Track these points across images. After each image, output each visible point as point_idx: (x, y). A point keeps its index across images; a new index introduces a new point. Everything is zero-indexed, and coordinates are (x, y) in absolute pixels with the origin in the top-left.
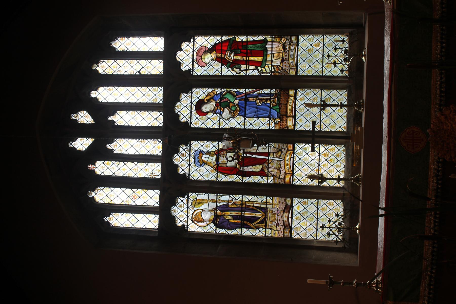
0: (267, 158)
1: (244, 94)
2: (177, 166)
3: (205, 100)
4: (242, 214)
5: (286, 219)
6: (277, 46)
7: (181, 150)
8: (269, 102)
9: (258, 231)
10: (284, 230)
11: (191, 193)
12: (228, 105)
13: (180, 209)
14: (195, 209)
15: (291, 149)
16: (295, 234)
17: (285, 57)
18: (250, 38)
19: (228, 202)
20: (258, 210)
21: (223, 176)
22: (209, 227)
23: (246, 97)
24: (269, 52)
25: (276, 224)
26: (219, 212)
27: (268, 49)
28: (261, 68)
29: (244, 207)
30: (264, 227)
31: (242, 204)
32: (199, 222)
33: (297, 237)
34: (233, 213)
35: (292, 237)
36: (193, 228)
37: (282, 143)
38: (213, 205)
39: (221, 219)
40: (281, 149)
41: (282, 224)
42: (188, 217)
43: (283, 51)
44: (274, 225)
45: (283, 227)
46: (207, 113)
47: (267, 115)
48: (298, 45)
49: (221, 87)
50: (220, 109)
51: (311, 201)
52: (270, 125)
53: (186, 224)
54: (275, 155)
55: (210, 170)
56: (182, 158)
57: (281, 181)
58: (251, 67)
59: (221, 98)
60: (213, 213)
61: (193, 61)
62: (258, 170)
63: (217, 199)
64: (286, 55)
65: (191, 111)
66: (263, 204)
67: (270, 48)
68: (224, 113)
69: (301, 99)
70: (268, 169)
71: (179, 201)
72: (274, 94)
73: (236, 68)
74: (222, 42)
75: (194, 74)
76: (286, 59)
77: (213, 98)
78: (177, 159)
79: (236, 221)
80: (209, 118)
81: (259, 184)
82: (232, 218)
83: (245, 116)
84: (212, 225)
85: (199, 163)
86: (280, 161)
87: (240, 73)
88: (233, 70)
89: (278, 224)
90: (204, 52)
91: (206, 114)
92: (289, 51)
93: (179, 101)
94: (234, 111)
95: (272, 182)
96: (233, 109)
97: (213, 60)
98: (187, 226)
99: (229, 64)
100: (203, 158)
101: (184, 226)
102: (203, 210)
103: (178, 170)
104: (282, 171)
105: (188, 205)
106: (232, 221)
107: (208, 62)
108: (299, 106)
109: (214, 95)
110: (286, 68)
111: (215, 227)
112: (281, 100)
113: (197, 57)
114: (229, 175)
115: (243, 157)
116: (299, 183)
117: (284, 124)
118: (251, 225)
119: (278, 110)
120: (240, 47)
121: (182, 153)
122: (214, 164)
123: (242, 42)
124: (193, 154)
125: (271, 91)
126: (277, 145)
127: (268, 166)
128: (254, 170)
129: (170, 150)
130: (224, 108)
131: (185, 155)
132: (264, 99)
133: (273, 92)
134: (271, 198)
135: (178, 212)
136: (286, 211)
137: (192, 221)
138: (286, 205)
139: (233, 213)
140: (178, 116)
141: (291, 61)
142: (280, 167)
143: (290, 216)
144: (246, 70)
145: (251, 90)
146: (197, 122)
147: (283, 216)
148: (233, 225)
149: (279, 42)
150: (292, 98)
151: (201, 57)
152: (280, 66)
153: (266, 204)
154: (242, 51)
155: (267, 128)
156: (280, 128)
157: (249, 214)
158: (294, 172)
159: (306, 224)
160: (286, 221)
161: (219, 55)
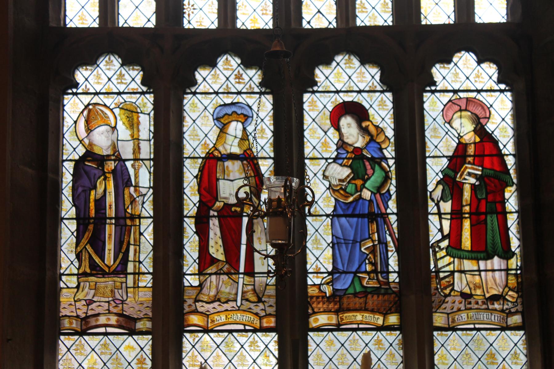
0: (242, 270)
1: (384, 211)
2: (213, 65)
3: (367, 123)
4: (111, 218)
5: (102, 320)
6: (498, 281)
7: (251, 72)
8: (369, 268)
9: (73, 256)
10: (78, 316)
11: (152, 100)
12: (359, 174)
13: (115, 77)
14: (117, 111)
15: (265, 325)
16: (68, 343)
17: (473, 301)
18: (512, 220)
19: (136, 186)
20: (121, 256)
21: (196, 172)
22: (75, 143)
23: (377, 217)
24: (482, 265)
25: (90, 297)
26: (111, 165)
27: (489, 262)
28: (447, 248)
29: (126, 222)
30: (81, 271)
31: (133, 217)
32: (87, 121)
33: (62, 349)
34: (111, 199)
35: (62, 337)
36: (73, 107)
37: (277, 303)
38: (127, 152)
39: (96, 172)
40: (263, 302)
41: (90, 313)
42: (96, 94)
43: (487, 295)
44: (87, 293)
45: (83, 316)
46: (338, 128)
47: (340, 267)
48: (503, 329)
49: (398, 159)
50: (349, 159)
52: (317, 273)
53: (80, 91)
54: (250, 288)
55: (208, 142)
56: (233, 76)
57: (190, 305)
58: (446, 225)
59: (373, 160)
60: (110, 152)
61: (455, 92)
62: (212, 251)
63: (142, 160)
64: (477, 303)
65: (341, 91)
66: (135, 266)
67: (492, 264)
68: (339, 168)
69: (379, 342)
70: (215, 274)
71: (134, 73)
72: (388, 279)
73: (443, 191)
74: (501, 156)
75: (426, 95)
76: (470, 303)
77: (372, 140)
78: (228, 64)
79: (92, 205)
80: (326, 133)
81: (179, 255)
82: (98, 197)
83: (335, 215)
84: (81, 151)
85: (221, 114)
86: (236, 301)
87: (433, 200)
88: (438, 183)
89: (89, 302)
90: (476, 116)
91: (336, 126)
92: (488, 309)
93: (363, 63)
94: (345, 190)
95: (186, 284)
96: (351, 188)
97: (460, 137)
98: (76, 94)
99: (452, 174)
100: (234, 124)
101: (76, 85)
102: (114, 128)
103: (204, 68)
104: (212, 305)
105: (124, 93)
106: (92, 197)
107: (454, 125)
108: (364, 337)
109: (378, 143)
110: (448, 305)
111: (77, 157)
112: (375, 297)
113: (465, 101)
114: (199, 184)
115: (240, 216)
116: (187, 346)
117: (320, 305)
118: (84, 241)
119: (351, 291)
120: (490, 198)
121: (244, 76)
122: (221, 149)
123: (503, 201)
124: (241, 100)
125: (395, 272)
126: (271, 291)
127: (224, 274)
128: (211, 243)
129: (249, 47)
130: (350, 167)
131: (239, 83)
132: (375, 256)
133: (393, 277)
134: (150, 285)
135: (107, 72)
136: (121, 319)
137: (89, 104)
138: (135, 320)
139: (111, 199)
140: (328, 62)
141: (464, 315)
142: (223, 300)
143: (110, 330)
144: (440, 214)
145: (395, 226)
146: (316, 108)
147: (110, 312)
148: (83, 200)
149: (506, 285)
150: (380, 322)
151: (466, 110)
152: (453, 289)
153: (134, 274)
154: (483, 203)
155: (308, 266)
156: (312, 297)
157: (110, 235)
158: (212, 335)
160: (97, 320)
161: (471, 150)
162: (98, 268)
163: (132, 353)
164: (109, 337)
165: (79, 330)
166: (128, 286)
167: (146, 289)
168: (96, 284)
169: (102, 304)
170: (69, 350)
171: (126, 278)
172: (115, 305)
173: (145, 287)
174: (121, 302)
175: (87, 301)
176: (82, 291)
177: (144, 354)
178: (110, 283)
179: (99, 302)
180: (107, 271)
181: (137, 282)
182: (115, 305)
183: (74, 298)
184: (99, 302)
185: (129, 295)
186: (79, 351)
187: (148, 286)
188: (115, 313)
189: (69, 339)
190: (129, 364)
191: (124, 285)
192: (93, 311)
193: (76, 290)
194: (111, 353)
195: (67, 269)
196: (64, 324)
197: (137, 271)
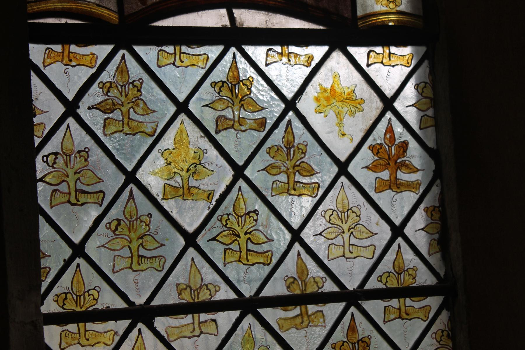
16: (70, 79)
51: (419, 219)
159: (185, 192)
163: (348, 120)
164: (250, 50)
165: (114, 17)
170: (71, 108)
177: (398, 128)
186: (117, 115)
189: (69, 60)
190: (343, 168)
194: (262, 123)
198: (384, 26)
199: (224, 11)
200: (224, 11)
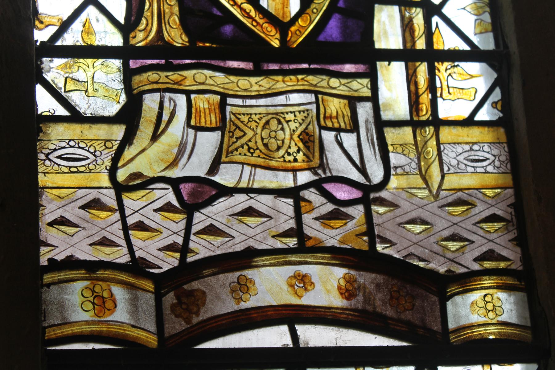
10: (137, 267)
25: (196, 166)
30: (139, 39)
41: (202, 248)
44: (176, 145)
45: (170, 262)
66: (407, 26)
89: (196, 194)
136: (365, 278)
160: (243, 287)
162: (228, 29)
165: (152, 340)
166: (386, 116)
167: (475, 133)
168: (223, 104)
169: (263, 203)
171: (372, 76)
172: (330, 207)
173: (469, 122)
174: (356, 194)
175: (185, 188)
176: (155, 137)
178: (295, 98)
179: (248, 191)
180: (276, 43)
181: (425, 98)
182: (330, 207)
183: (112, 172)
184: (248, 191)
185: (395, 159)
187: (479, 117)
188: (332, 250)
191: (364, 111)
192: (218, 240)
193: (118, 132)
195: (65, 26)
196: (62, 306)
197: (421, 44)
198: (483, 341)
199: (285, 328)
200: (285, 328)
